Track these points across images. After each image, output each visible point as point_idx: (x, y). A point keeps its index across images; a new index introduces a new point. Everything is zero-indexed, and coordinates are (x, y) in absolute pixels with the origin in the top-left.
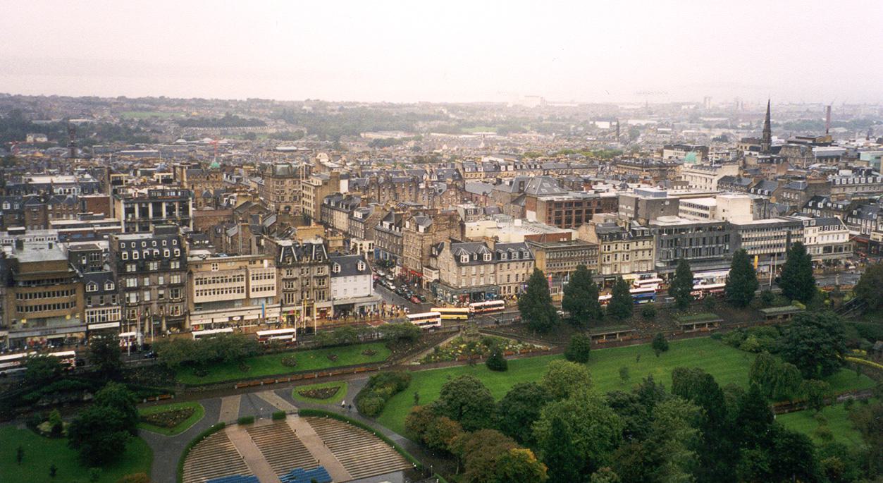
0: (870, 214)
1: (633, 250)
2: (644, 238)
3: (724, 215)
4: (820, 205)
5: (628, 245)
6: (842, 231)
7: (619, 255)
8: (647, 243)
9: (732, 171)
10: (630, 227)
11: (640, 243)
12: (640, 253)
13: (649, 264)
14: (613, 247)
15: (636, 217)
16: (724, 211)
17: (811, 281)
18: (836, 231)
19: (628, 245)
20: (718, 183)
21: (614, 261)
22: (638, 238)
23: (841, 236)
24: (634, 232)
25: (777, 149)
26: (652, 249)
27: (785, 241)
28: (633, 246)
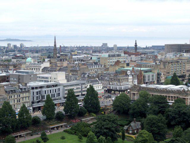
0: (106, 78)
1: (21, 98)
2: (26, 92)
3: (55, 80)
4: (86, 76)
5: (19, 95)
6: (100, 85)
7: (15, 100)
8: (27, 93)
9: (47, 64)
10: (19, 87)
11: (24, 94)
12: (24, 99)
13: (29, 103)
14: (13, 97)
15: (19, 82)
16: (55, 78)
17: (98, 103)
18: (98, 85)
19: (19, 95)
20: (42, 70)
21: (14, 103)
22: (23, 92)
23: (99, 87)
24: (21, 89)
25: (59, 57)
26: (29, 97)
27: (80, 90)
28: (22, 95)
